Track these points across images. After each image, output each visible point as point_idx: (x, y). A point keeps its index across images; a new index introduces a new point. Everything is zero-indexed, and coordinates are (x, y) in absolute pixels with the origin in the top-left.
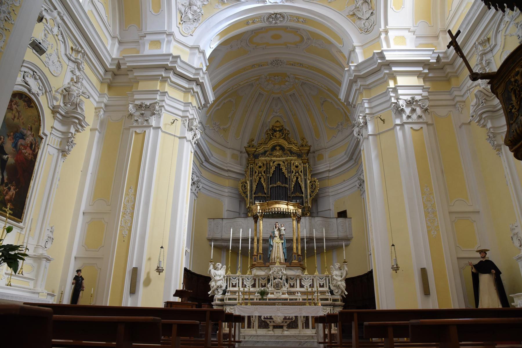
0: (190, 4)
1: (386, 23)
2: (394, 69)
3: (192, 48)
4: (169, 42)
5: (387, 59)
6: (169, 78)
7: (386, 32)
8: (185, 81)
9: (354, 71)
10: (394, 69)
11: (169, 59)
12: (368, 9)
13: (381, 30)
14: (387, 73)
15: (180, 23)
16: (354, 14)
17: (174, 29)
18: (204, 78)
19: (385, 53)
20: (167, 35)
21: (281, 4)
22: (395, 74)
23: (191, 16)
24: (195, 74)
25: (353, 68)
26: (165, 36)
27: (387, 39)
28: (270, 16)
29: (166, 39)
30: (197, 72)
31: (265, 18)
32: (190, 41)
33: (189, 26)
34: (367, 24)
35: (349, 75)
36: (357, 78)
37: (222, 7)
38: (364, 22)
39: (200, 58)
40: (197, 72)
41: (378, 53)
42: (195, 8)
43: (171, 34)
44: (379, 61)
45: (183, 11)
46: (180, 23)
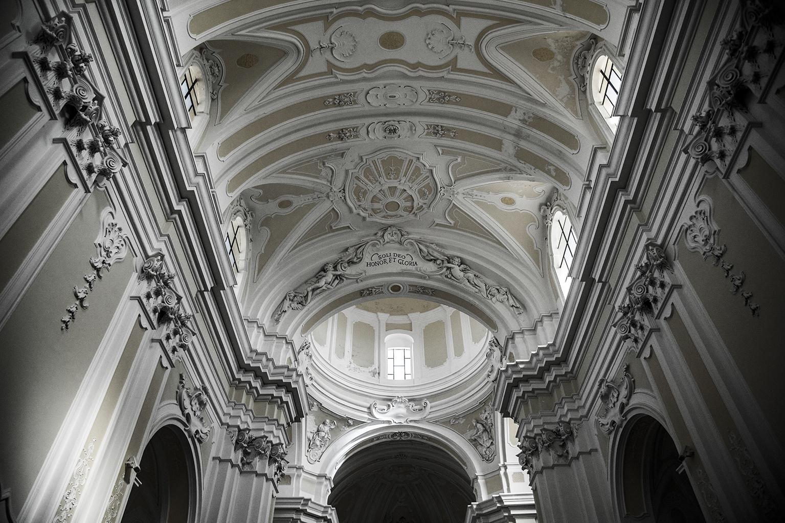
0: (318, 431)
1: (505, 460)
2: (513, 512)
3: (319, 476)
4: (299, 476)
5: (505, 504)
6: (300, 520)
7: (505, 467)
8: (313, 519)
9: (476, 509)
10: (513, 512)
11: (300, 503)
12: (488, 439)
13: (500, 465)
14: (506, 516)
15: (308, 451)
16: (475, 440)
17: (304, 463)
18: (332, 514)
19: (503, 498)
20: (297, 468)
21: (406, 424)
22: (514, 517)
23: (318, 443)
24: (323, 512)
25: (475, 507)
26: (295, 469)
27: (506, 474)
28: (395, 434)
29: (296, 473)
30: (326, 510)
31: (390, 436)
32: (316, 469)
33: (316, 452)
34: (487, 452)
35: (472, 511)
36: (478, 517)
37: (347, 429)
38: (485, 449)
39: (326, 486)
40: (326, 510)
41: (496, 497)
42: (323, 434)
43: (300, 468)
44: (498, 505)
45: (311, 438)
46: (308, 451)
